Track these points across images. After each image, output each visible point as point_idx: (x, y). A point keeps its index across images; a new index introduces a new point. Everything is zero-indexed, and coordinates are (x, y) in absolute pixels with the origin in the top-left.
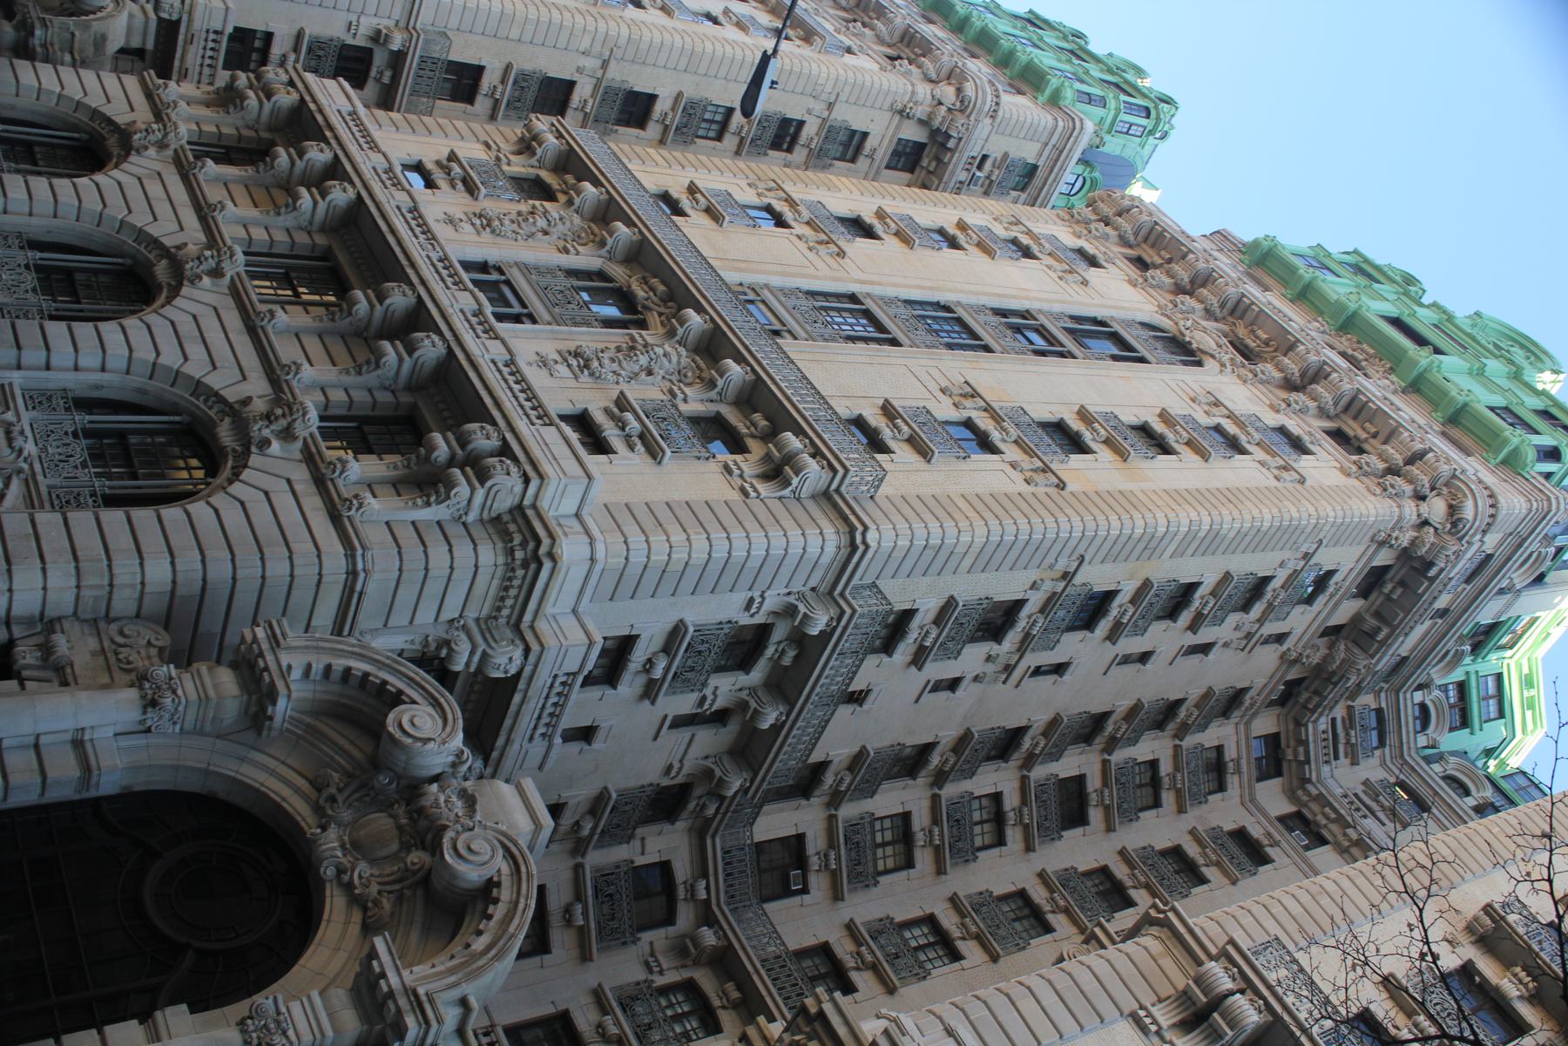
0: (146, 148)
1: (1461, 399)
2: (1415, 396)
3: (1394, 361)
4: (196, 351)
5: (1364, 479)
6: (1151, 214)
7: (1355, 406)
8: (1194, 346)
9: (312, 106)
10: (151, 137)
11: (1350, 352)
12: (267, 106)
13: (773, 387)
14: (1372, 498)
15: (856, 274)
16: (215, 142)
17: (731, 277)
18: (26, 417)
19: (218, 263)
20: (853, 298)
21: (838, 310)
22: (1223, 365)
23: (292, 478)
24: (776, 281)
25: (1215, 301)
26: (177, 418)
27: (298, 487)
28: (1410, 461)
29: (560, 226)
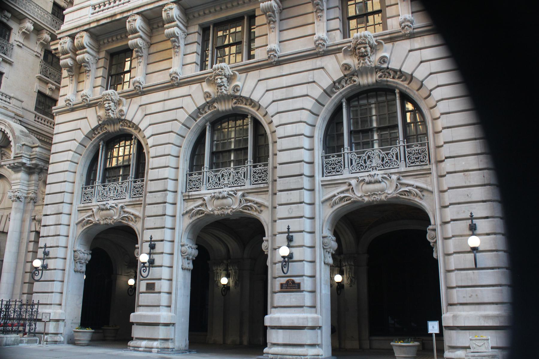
0: (121, 111)
4: (298, 91)
9: (92, 25)
10: (113, 108)
12: (88, 49)
16: (106, 80)
18: (94, 203)
19: (225, 76)
23: (409, 49)
26: (101, 146)
27: (417, 46)
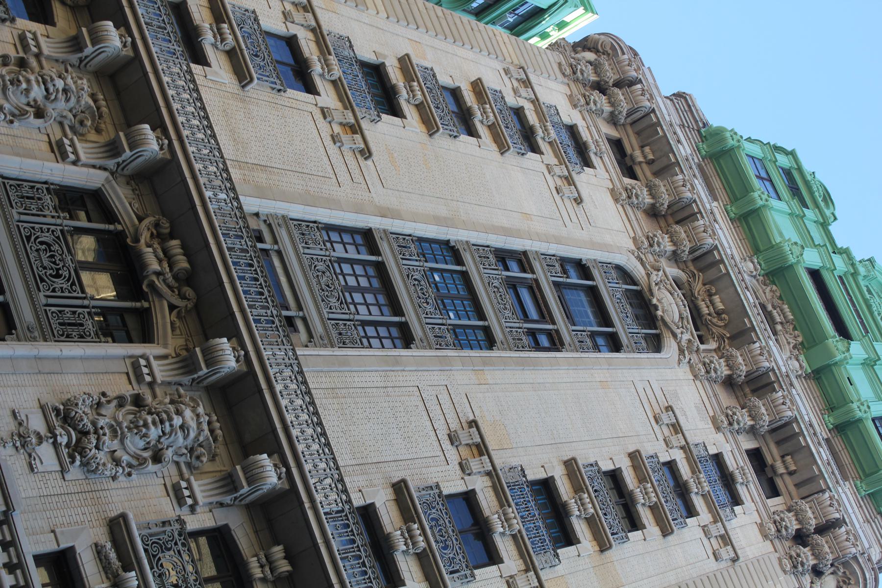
1: (859, 414)
2: (812, 384)
3: (809, 342)
5: (776, 542)
6: (651, 98)
7: (784, 433)
8: (659, 313)
11: (770, 308)
13: (310, 514)
14: (782, 577)
15: (380, 196)
17: (250, 204)
20: (368, 238)
21: (352, 262)
22: (681, 351)
24: (297, 211)
25: (687, 246)
28: (822, 530)
29: (61, 105)
